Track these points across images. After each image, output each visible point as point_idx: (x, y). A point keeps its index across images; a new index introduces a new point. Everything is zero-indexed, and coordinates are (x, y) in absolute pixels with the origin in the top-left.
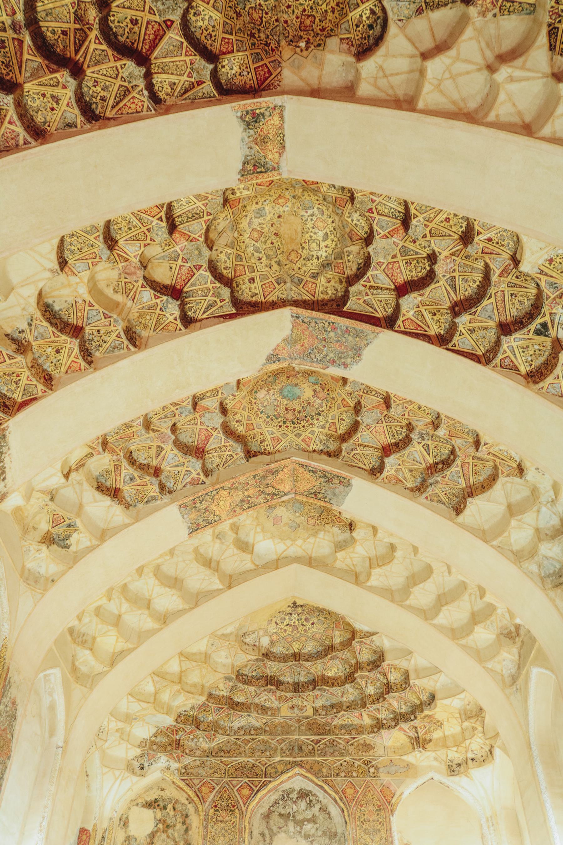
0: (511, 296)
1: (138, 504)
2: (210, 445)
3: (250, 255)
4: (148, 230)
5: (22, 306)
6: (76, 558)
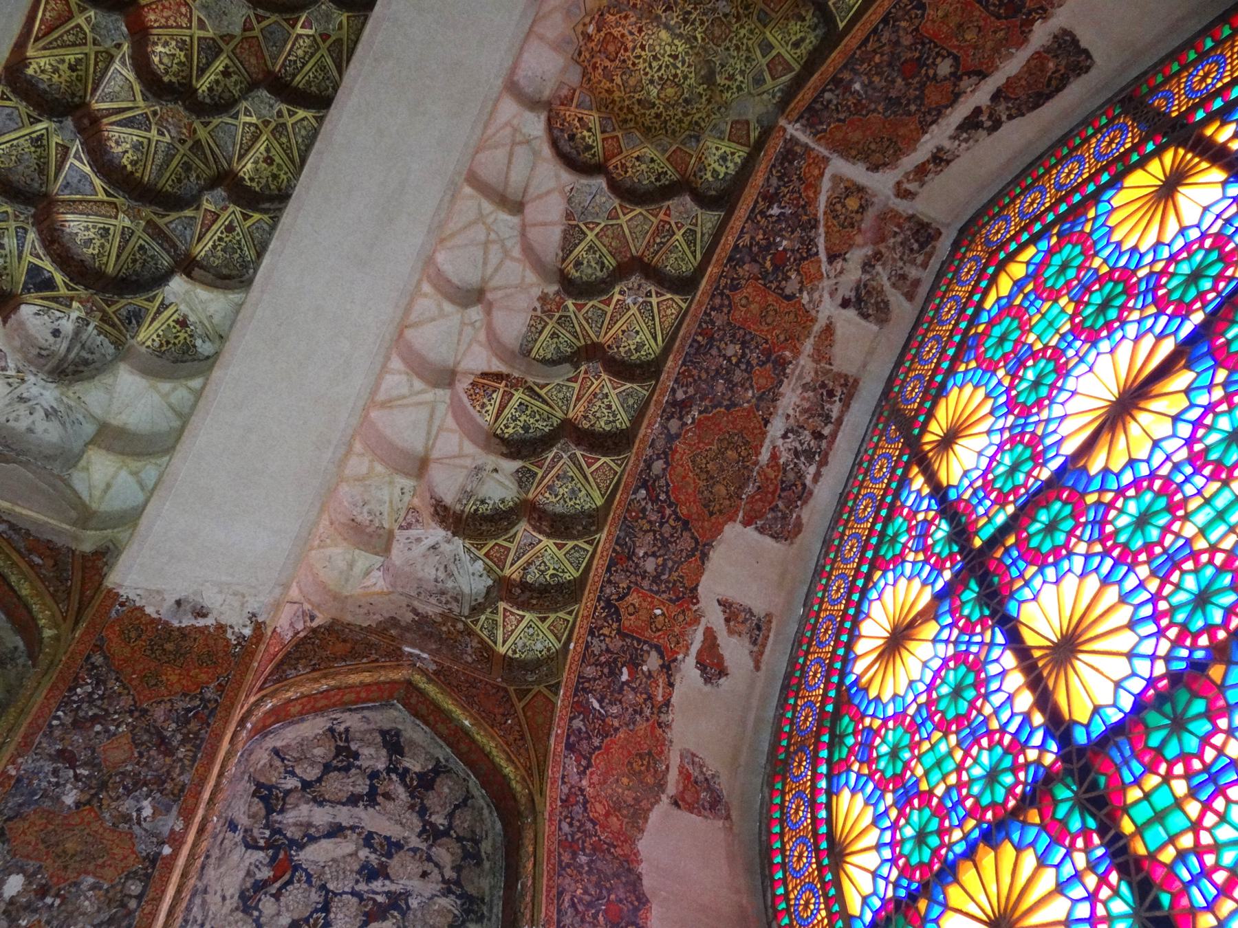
0: (104, 228)
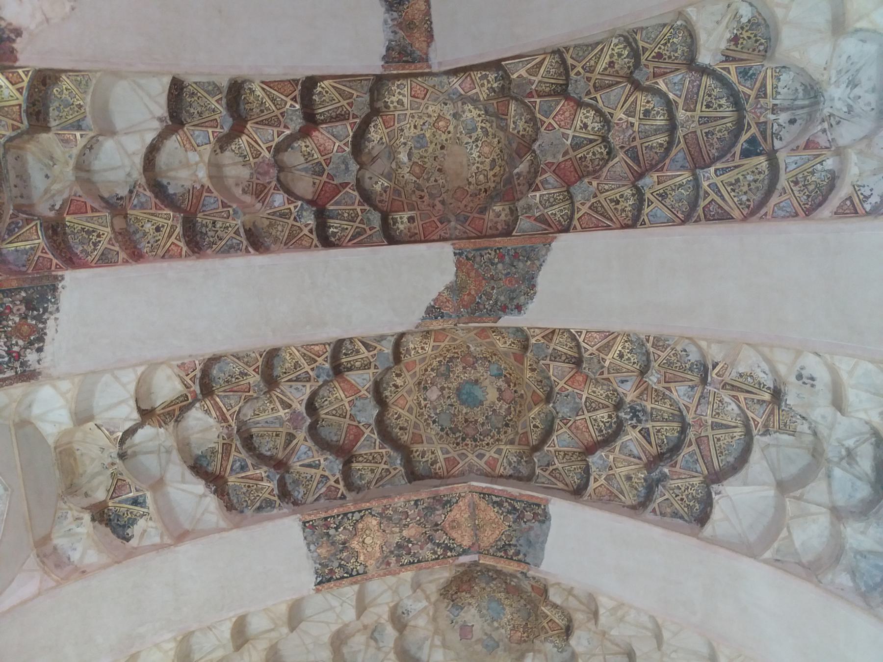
0: (707, 136)
1: (246, 510)
2: (360, 448)
3: (410, 191)
4: (281, 114)
5: (128, 170)
6: (131, 554)
